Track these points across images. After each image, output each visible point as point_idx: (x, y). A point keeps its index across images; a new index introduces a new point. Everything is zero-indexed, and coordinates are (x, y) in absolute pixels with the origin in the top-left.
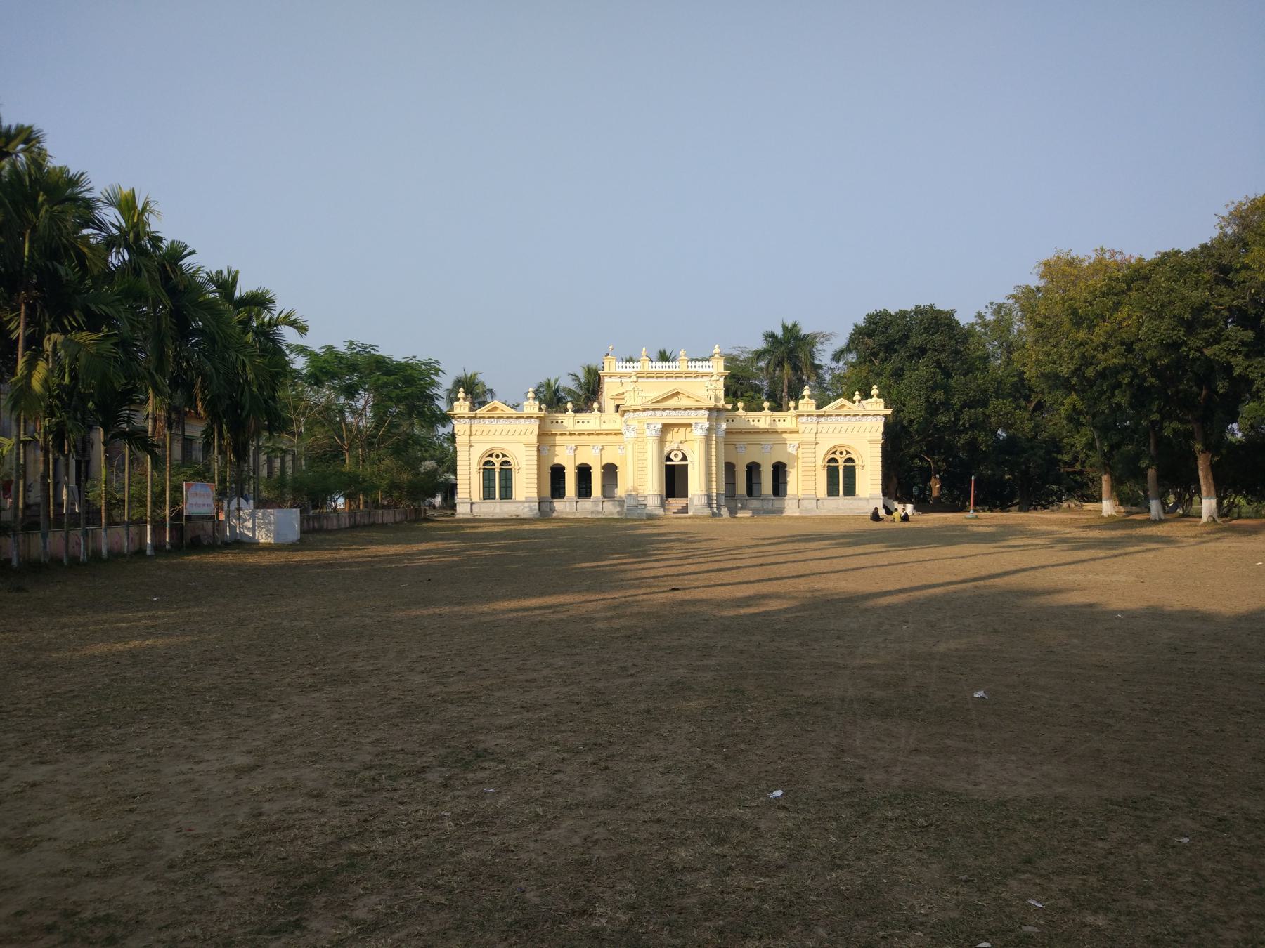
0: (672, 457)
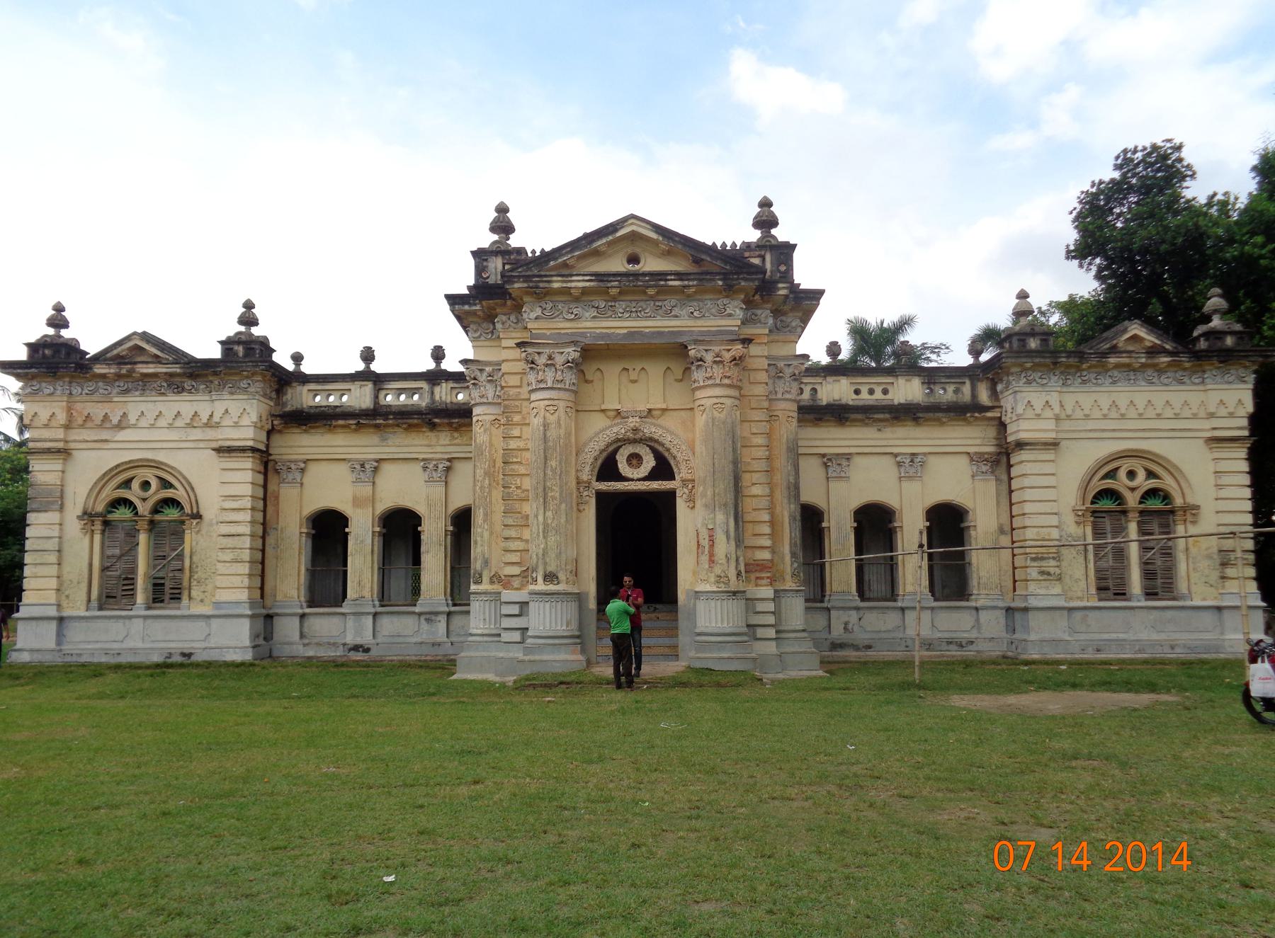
0: (623, 468)
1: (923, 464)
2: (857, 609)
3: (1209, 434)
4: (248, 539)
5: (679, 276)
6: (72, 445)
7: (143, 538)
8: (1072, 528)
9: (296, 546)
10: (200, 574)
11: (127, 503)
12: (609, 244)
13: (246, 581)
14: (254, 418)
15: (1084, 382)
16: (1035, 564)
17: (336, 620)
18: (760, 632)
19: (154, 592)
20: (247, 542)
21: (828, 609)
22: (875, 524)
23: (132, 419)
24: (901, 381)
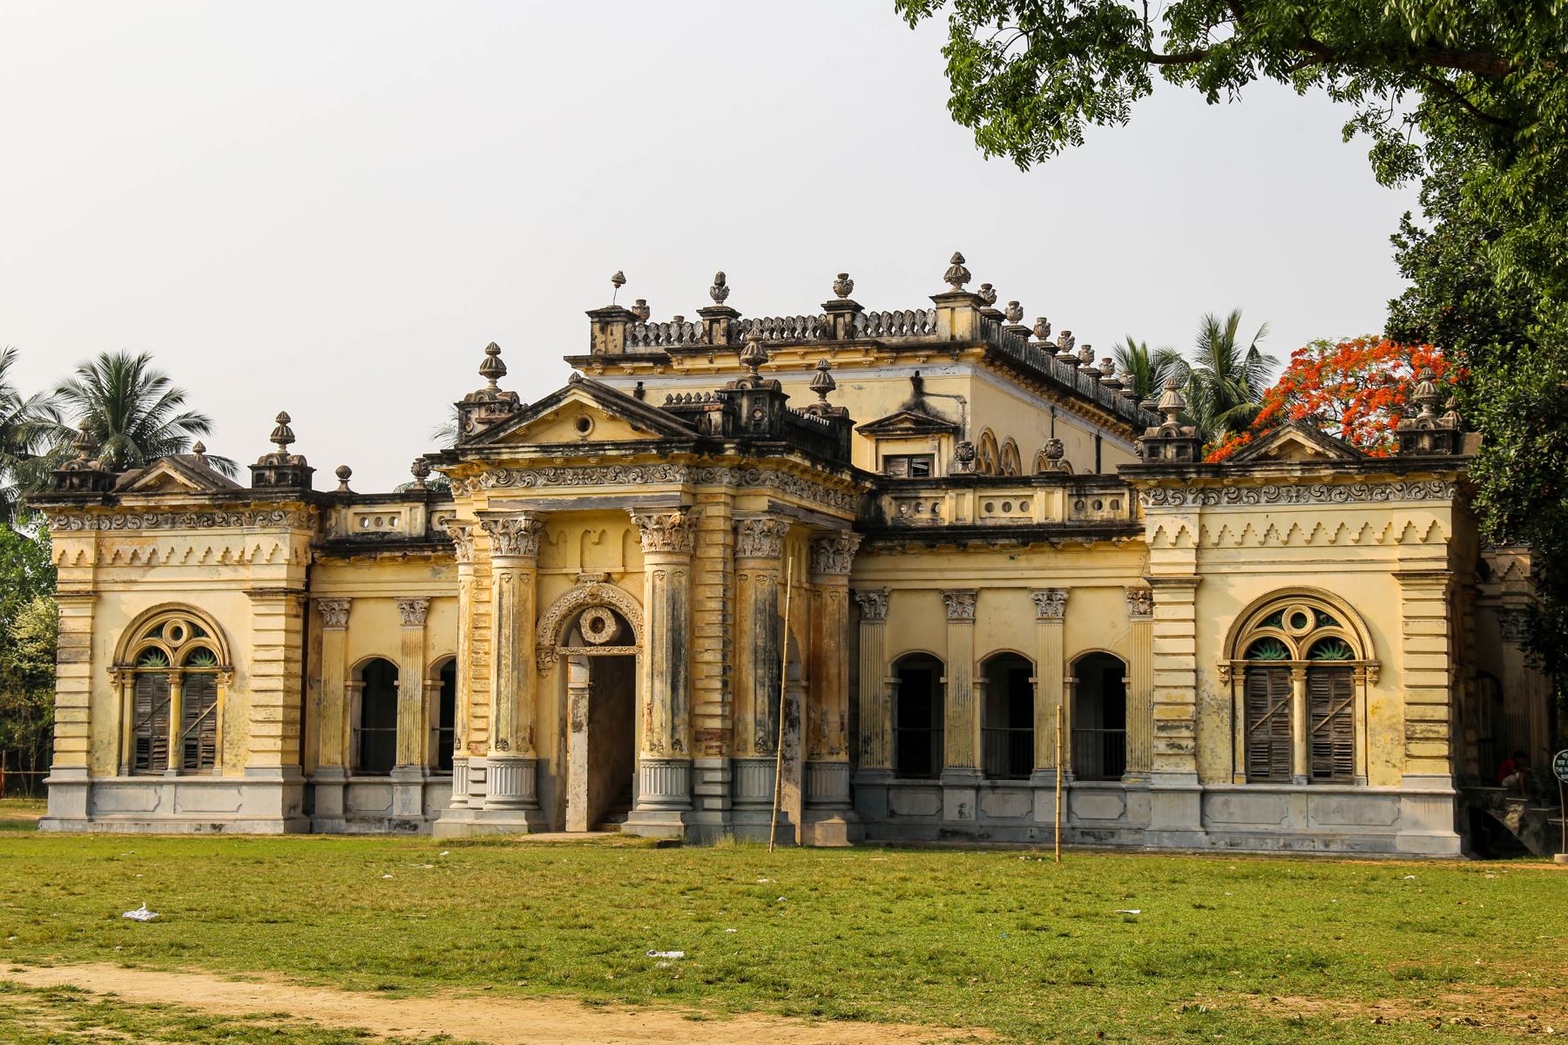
0: (588, 634)
1: (1066, 602)
2: (978, 788)
3: (1397, 567)
4: (281, 695)
5: (617, 445)
6: (102, 587)
7: (174, 692)
8: (1216, 687)
9: (340, 703)
10: (232, 735)
11: (155, 652)
12: (556, 413)
13: (279, 742)
14: (285, 553)
15: (1232, 501)
16: (1163, 734)
17: (382, 791)
18: (708, 803)
19: (187, 756)
20: (279, 699)
21: (941, 788)
22: (1009, 677)
23: (162, 556)
24: (1040, 495)
